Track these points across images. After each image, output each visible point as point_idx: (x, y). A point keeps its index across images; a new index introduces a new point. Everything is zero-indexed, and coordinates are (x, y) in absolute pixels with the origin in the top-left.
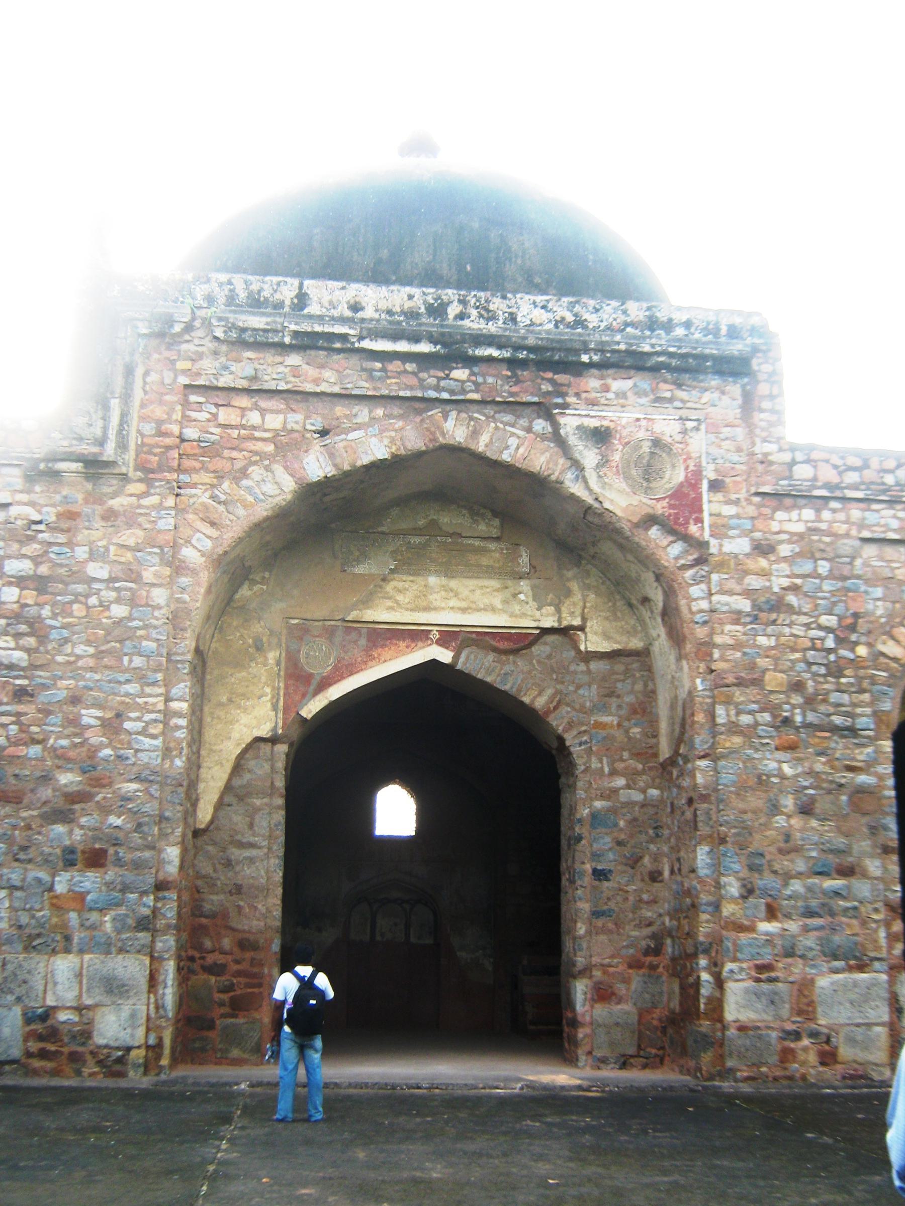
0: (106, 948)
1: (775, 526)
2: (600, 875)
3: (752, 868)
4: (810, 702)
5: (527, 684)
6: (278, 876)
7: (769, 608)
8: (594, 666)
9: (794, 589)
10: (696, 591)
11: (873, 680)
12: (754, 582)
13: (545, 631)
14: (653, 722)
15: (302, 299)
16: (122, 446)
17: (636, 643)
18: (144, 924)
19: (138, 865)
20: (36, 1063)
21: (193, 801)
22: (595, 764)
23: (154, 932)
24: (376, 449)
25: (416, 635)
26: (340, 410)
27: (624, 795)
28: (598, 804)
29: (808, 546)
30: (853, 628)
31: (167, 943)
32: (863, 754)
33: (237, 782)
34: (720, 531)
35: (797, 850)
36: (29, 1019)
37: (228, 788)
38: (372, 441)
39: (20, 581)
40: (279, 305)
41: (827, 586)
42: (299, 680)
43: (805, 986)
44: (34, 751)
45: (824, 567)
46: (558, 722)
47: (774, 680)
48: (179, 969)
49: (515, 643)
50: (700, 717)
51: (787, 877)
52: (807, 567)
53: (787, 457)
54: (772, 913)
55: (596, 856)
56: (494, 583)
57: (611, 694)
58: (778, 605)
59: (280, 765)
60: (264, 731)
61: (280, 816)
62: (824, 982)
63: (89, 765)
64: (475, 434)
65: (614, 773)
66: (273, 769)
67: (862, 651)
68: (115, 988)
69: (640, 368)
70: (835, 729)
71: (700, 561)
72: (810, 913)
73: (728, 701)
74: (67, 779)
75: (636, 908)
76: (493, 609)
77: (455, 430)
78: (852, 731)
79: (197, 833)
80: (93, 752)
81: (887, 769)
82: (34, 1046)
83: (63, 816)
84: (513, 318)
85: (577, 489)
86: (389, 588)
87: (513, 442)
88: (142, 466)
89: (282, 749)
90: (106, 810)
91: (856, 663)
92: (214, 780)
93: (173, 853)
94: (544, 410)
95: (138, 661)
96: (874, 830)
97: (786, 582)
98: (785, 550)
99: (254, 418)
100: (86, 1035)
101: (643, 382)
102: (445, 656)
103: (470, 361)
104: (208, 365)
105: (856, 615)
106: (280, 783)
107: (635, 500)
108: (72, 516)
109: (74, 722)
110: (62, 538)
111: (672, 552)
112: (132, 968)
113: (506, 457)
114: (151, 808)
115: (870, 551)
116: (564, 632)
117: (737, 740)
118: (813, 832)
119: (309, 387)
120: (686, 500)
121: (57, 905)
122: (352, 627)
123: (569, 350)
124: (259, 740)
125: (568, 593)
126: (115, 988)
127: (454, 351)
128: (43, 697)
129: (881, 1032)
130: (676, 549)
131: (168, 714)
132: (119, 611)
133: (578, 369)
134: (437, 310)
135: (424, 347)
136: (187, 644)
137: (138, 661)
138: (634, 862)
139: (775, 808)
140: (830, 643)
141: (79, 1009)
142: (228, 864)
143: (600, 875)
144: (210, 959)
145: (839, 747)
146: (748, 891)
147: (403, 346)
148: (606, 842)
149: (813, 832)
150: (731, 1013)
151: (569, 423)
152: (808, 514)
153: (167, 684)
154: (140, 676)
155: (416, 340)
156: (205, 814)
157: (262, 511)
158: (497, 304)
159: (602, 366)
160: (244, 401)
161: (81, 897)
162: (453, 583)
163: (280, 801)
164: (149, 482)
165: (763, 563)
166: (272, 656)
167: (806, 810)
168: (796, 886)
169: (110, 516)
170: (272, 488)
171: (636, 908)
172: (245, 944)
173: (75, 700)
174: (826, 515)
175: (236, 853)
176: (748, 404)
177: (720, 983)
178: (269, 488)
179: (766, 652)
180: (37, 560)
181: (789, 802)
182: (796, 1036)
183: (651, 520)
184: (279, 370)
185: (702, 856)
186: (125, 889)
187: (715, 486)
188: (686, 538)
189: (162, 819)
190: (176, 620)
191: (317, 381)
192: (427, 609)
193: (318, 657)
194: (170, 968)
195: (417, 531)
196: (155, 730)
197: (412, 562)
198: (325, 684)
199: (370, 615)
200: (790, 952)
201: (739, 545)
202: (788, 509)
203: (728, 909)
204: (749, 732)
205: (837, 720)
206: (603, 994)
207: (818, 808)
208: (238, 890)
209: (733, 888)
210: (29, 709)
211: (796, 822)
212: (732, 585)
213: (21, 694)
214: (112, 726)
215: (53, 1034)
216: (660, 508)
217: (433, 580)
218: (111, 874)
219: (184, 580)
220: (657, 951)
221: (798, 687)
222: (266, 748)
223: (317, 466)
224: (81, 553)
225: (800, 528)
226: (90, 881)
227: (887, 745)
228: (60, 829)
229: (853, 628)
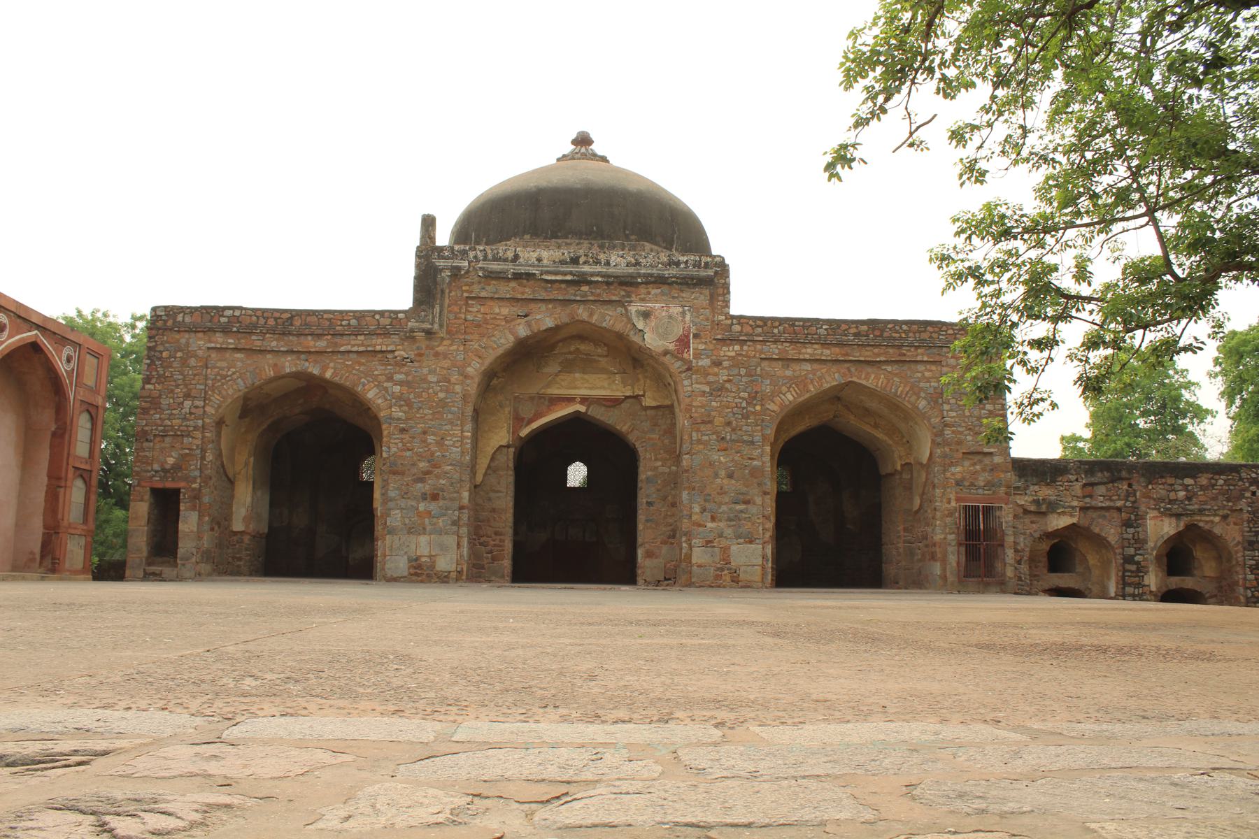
0: (440, 532)
1: (722, 353)
2: (649, 504)
3: (705, 501)
4: (733, 430)
6: (511, 504)
8: (649, 412)
9: (729, 381)
10: (686, 383)
11: (763, 421)
12: (711, 378)
13: (627, 397)
14: (675, 437)
15: (516, 257)
16: (441, 326)
17: (668, 402)
18: (454, 523)
19: (451, 499)
20: (414, 578)
21: (473, 473)
22: (648, 456)
23: (459, 526)
24: (549, 323)
25: (570, 400)
26: (532, 306)
27: (661, 469)
28: (649, 473)
29: (736, 362)
30: (754, 398)
31: (464, 530)
32: (757, 453)
33: (493, 465)
34: (697, 355)
35: (725, 493)
36: (410, 560)
37: (489, 467)
38: (545, 319)
39: (401, 383)
40: (506, 260)
41: (744, 379)
42: (519, 421)
43: (725, 550)
44: (408, 453)
45: (743, 371)
46: (632, 438)
47: (718, 421)
48: (469, 543)
49: (614, 402)
50: (686, 437)
51: (720, 504)
52: (735, 371)
53: (729, 322)
54: (713, 519)
55: (648, 496)
56: (604, 376)
57: (656, 425)
58: (722, 388)
59: (511, 457)
60: (504, 443)
61: (511, 479)
62: (734, 548)
64: (591, 315)
65: (656, 459)
66: (508, 458)
67: (758, 408)
68: (444, 548)
69: (664, 283)
70: (744, 442)
71: (688, 369)
72: (730, 520)
73: (698, 431)
74: (422, 465)
75: (665, 518)
76: (603, 388)
77: (582, 313)
78: (752, 443)
79: (476, 487)
80: (432, 454)
81: (767, 459)
82: (412, 571)
83: (421, 480)
84: (608, 263)
85: (636, 339)
86: (557, 379)
87: (608, 318)
88: (449, 332)
89: (512, 450)
90: (438, 477)
91: (756, 413)
92: (483, 463)
93: (466, 495)
94: (619, 303)
95: (450, 416)
96: (759, 485)
97: (725, 378)
98: (726, 364)
99: (497, 310)
100: (432, 567)
101: (665, 288)
102: (582, 409)
103: (589, 283)
104: (476, 288)
105: (756, 392)
106: (511, 465)
107: (660, 343)
108: (420, 355)
109: (424, 441)
110: (416, 364)
111: (676, 366)
112: (451, 540)
113: (604, 325)
114: (456, 476)
115: (765, 364)
116: (636, 397)
117: (701, 447)
118: (733, 486)
119: (519, 296)
121: (420, 515)
122: (541, 397)
123: (632, 277)
124: (501, 446)
125: (638, 380)
126: (444, 548)
127: (581, 280)
128: (412, 431)
129: (759, 568)
130: (680, 363)
131: (462, 437)
132: (441, 395)
133: (637, 285)
134: (575, 261)
135: (569, 278)
136: (469, 410)
137: (450, 416)
138: (664, 499)
139: (716, 475)
140: (744, 404)
141: (430, 556)
142: (490, 499)
143: (649, 504)
144: (482, 540)
145: (746, 450)
146: (704, 510)
147: (559, 278)
148: (653, 489)
149: (733, 486)
150: (694, 561)
151: (633, 309)
152: (737, 348)
153: (462, 426)
154: (451, 423)
155: (565, 274)
156: (479, 478)
157: (500, 351)
158: (602, 257)
159: (646, 283)
160: (491, 303)
161: (429, 512)
162: (586, 376)
163: (511, 473)
164: (453, 340)
165: (716, 370)
166: (507, 410)
167: (730, 476)
168: (724, 508)
169: (437, 355)
170: (504, 341)
171: (665, 518)
172: (496, 533)
173: (425, 433)
174: (745, 348)
175: (492, 495)
176: (712, 298)
177: (691, 547)
178: (502, 341)
179: (715, 409)
180: (407, 374)
181: (723, 473)
182: (722, 570)
183: (666, 353)
184: (505, 289)
185: (685, 495)
186: (447, 509)
187: (696, 336)
188: (682, 359)
189: (461, 480)
190: (465, 397)
191: (523, 293)
192: (575, 388)
193: (526, 410)
194: (465, 541)
195: (570, 353)
196: (458, 444)
197: (568, 367)
198: (530, 422)
199: (549, 391)
200: (720, 536)
201: (705, 362)
202: (728, 346)
203: (694, 518)
204: (706, 444)
205: (745, 438)
206: (649, 554)
207: (735, 476)
208: (494, 510)
209: (697, 509)
210: (406, 437)
211: (726, 481)
212: (702, 379)
213: (403, 430)
214: (441, 443)
215: (419, 567)
216: (672, 347)
217: (577, 375)
218: (441, 503)
219: (468, 381)
220: (674, 537)
221: (729, 423)
222: (505, 450)
223: (523, 331)
224: (425, 371)
225: (733, 354)
226: (433, 506)
227: (768, 449)
228: (420, 485)
229: (754, 398)
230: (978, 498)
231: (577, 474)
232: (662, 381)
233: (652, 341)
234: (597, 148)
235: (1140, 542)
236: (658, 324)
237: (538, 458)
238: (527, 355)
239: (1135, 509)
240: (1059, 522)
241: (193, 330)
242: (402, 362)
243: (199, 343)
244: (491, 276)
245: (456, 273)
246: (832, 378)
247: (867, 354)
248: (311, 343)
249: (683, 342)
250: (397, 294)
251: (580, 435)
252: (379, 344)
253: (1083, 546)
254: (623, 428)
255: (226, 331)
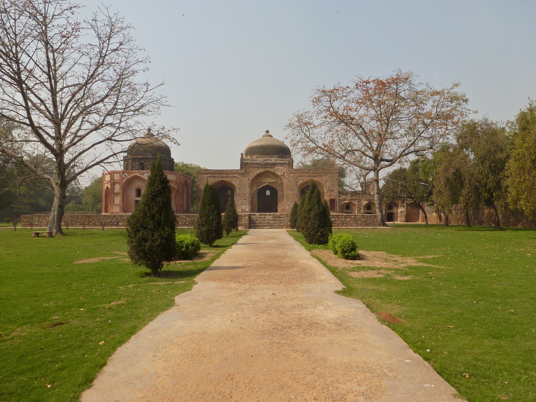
5: (274, 186)
7: (290, 181)
38: (262, 170)
42: (258, 186)
49: (273, 183)
63: (244, 193)
77: (268, 169)
120: (284, 174)
127: (267, 164)
149: (292, 197)
170: (256, 174)
184: (255, 166)
197: (266, 177)
223: (258, 173)
230: (332, 198)
231: (268, 193)
232: (281, 179)
233: (279, 173)
234: (270, 133)
235: (360, 205)
236: (280, 171)
237: (261, 192)
238: (259, 175)
239: (360, 199)
240: (346, 202)
241: (204, 174)
242: (239, 178)
243: (205, 176)
244: (252, 163)
245: (247, 163)
246: (309, 179)
247: (314, 175)
248: (224, 175)
249: (284, 174)
250: (237, 167)
251: (268, 187)
252: (235, 175)
253: (352, 205)
254: (275, 187)
255: (210, 174)
